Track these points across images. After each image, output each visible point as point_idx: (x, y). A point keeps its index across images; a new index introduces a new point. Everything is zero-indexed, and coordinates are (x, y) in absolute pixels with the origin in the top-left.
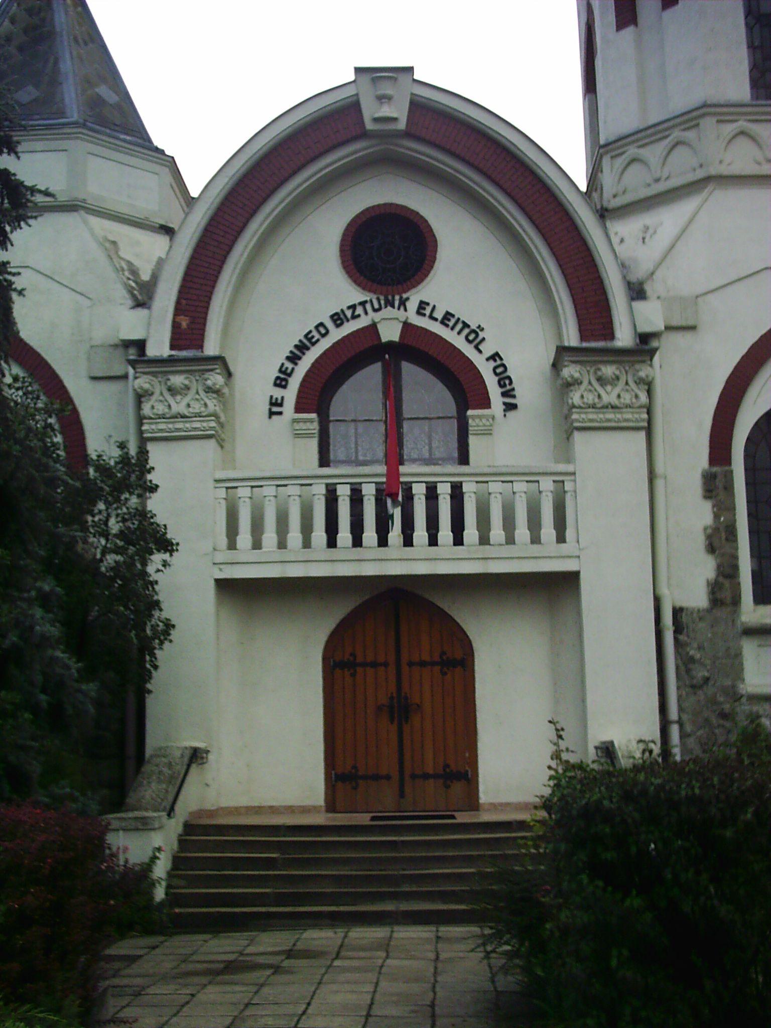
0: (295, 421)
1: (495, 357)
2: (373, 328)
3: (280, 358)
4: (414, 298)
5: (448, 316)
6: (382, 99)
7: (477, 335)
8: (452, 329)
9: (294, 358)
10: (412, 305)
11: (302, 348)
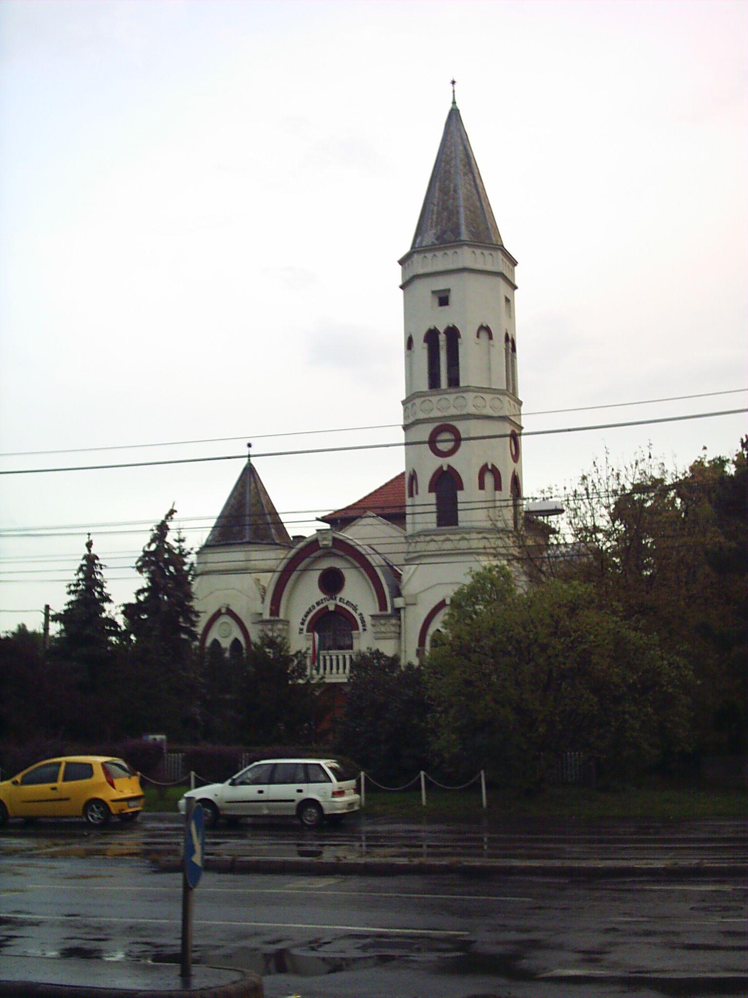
0: (306, 635)
2: (327, 607)
3: (302, 616)
4: (339, 596)
5: (348, 602)
6: (325, 539)
9: (306, 616)
10: (338, 599)
11: (308, 613)
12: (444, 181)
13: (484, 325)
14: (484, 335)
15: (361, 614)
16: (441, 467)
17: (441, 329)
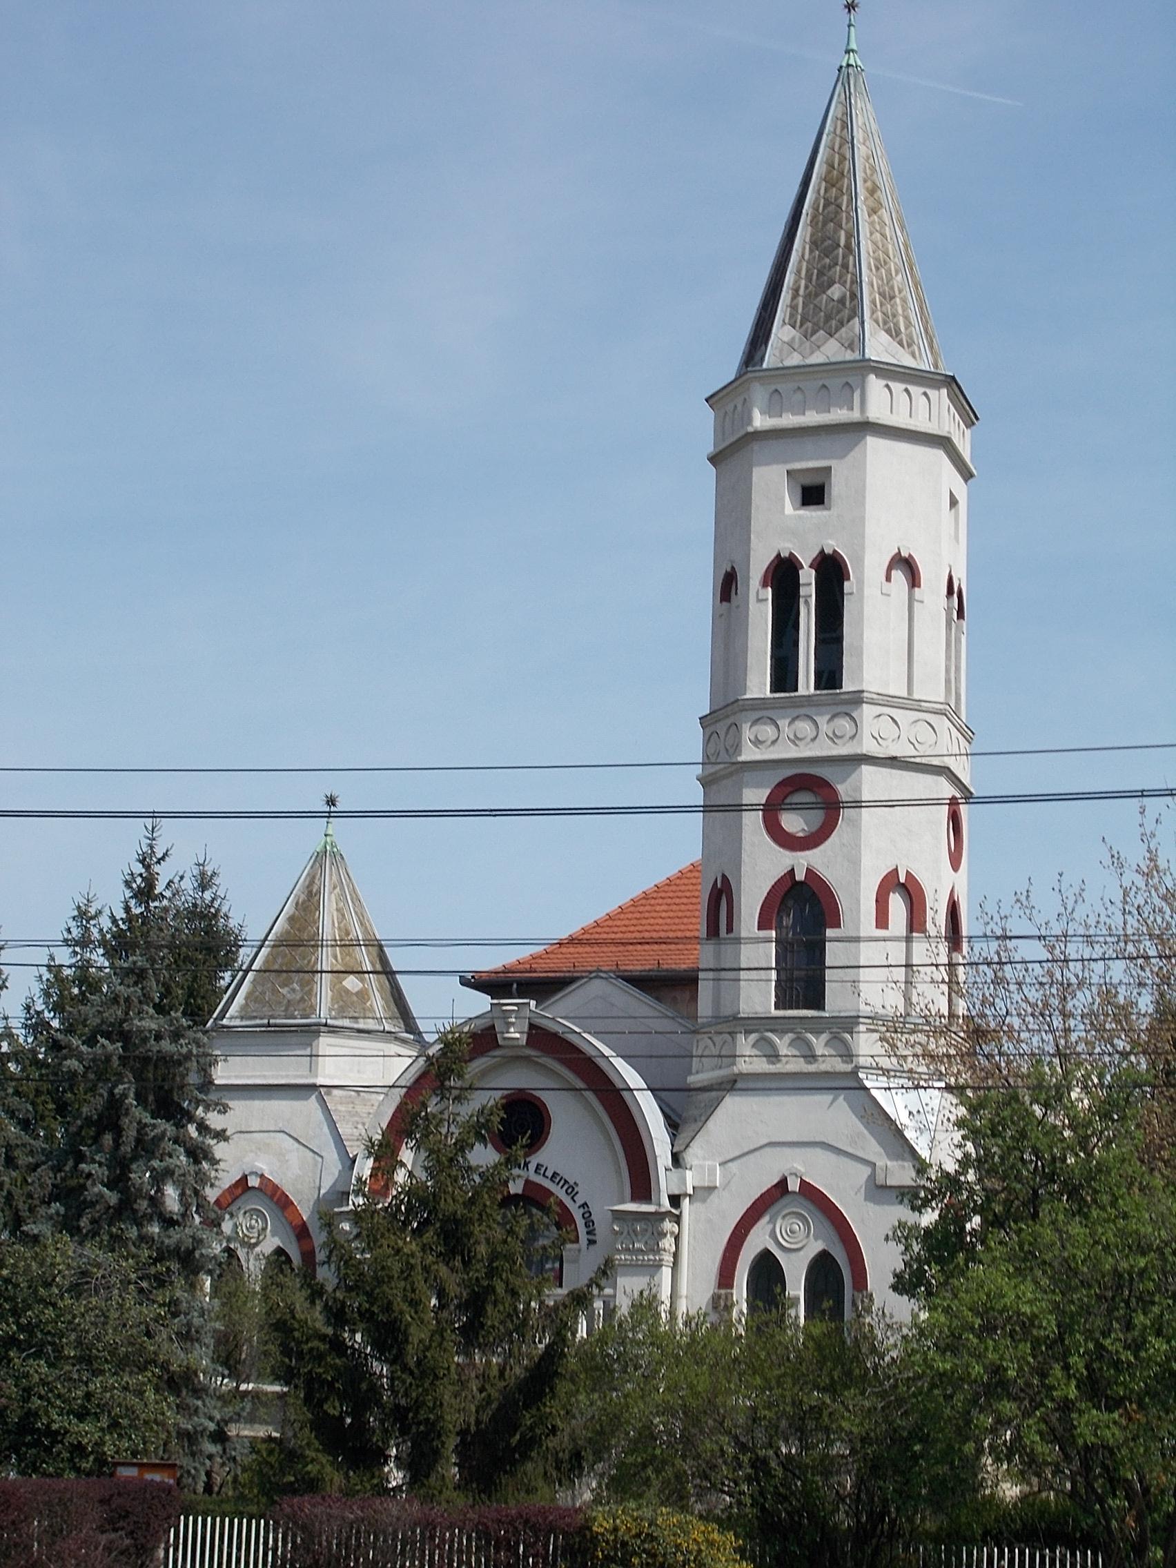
1: (585, 1205)
4: (534, 1161)
7: (573, 1189)
8: (558, 1183)
10: (532, 1167)
12: (825, 224)
13: (904, 554)
14: (899, 576)
15: (585, 1205)
16: (792, 872)
17: (805, 559)
